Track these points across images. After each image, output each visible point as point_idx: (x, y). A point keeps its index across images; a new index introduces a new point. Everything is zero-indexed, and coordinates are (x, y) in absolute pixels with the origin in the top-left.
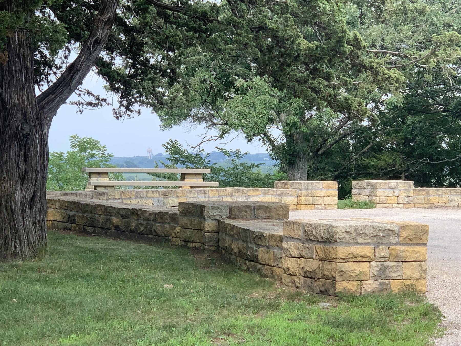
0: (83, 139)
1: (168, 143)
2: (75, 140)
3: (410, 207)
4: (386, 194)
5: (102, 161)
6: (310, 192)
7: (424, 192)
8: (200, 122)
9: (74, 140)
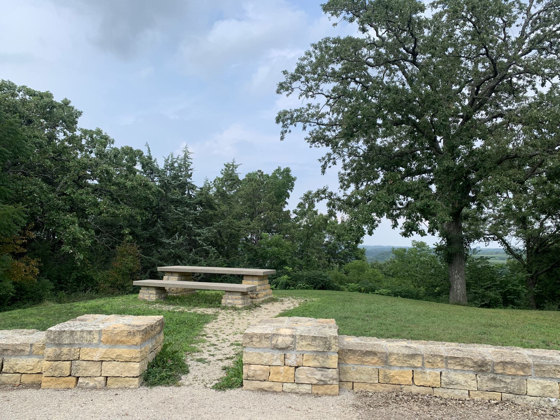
3: (328, 392)
4: (265, 360)
6: (65, 350)
7: (376, 359)
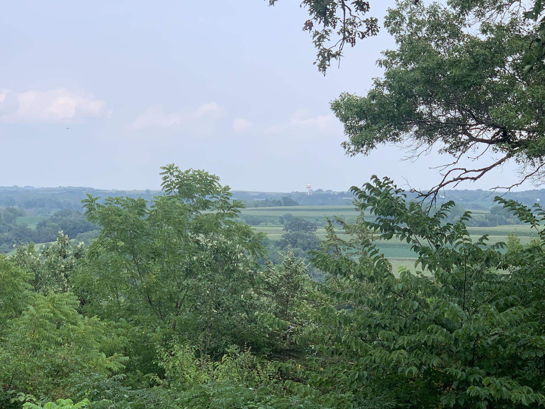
0: (187, 172)
1: (369, 186)
2: (172, 174)
5: (223, 215)
8: (431, 139)
9: (169, 174)
